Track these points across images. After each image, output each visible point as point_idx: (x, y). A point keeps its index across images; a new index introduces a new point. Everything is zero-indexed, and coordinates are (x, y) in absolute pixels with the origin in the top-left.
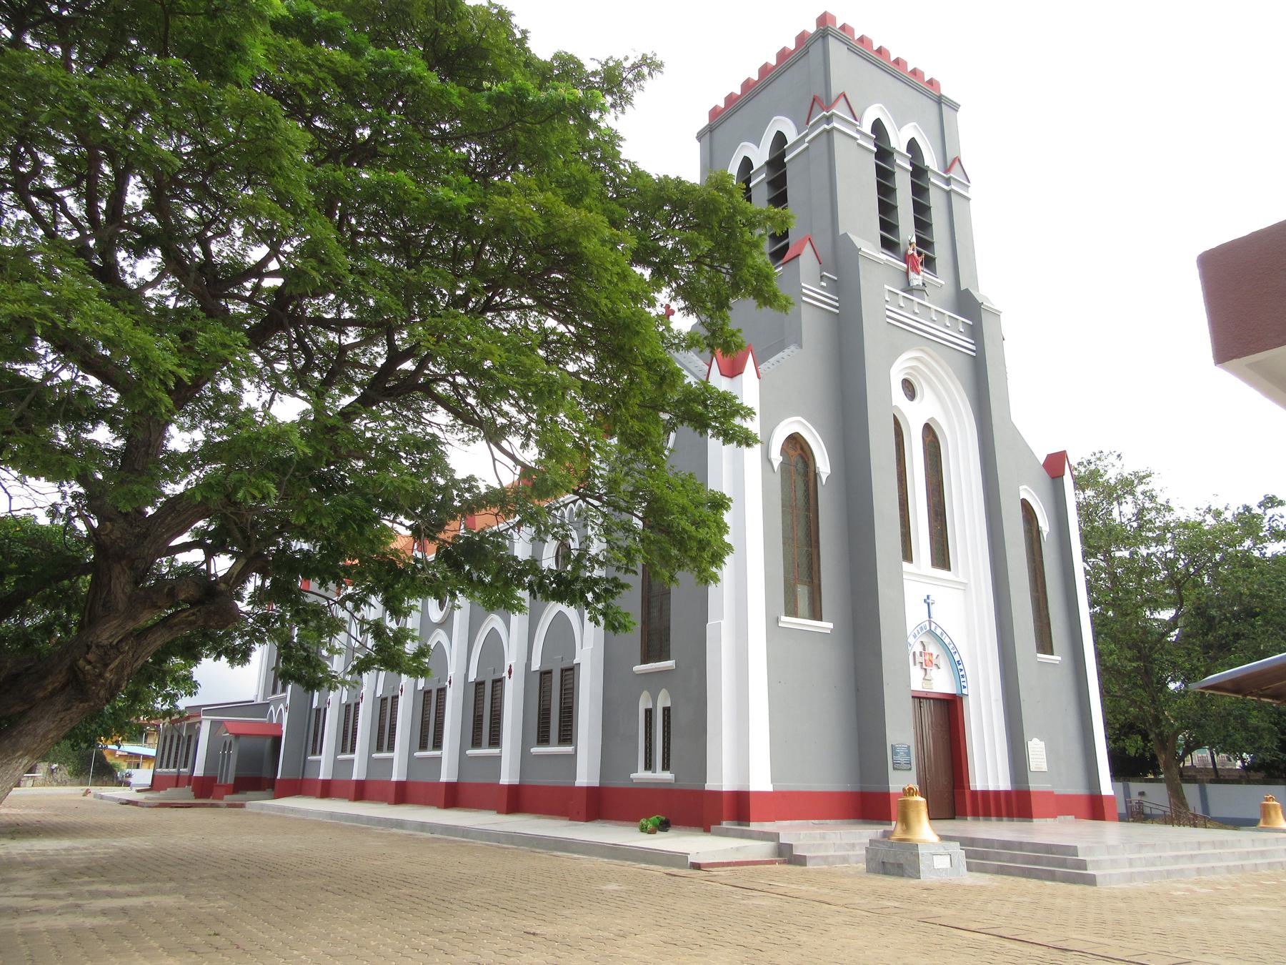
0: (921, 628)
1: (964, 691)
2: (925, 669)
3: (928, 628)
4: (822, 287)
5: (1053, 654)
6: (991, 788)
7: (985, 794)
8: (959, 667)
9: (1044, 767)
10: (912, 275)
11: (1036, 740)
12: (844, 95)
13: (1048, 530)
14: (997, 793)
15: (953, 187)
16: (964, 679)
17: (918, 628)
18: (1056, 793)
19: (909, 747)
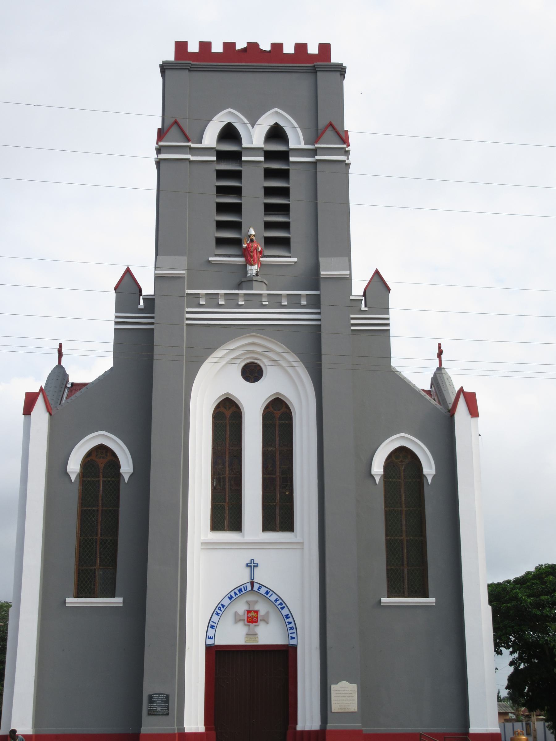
0: (240, 591)
1: (293, 642)
2: (249, 625)
3: (249, 588)
4: (141, 311)
5: (428, 597)
6: (307, 728)
7: (302, 732)
8: (287, 621)
9: (353, 707)
10: (249, 267)
11: (344, 684)
12: (176, 122)
13: (433, 472)
14: (309, 733)
15: (318, 157)
16: (294, 631)
17: (236, 591)
18: (364, 732)
19: (168, 697)
